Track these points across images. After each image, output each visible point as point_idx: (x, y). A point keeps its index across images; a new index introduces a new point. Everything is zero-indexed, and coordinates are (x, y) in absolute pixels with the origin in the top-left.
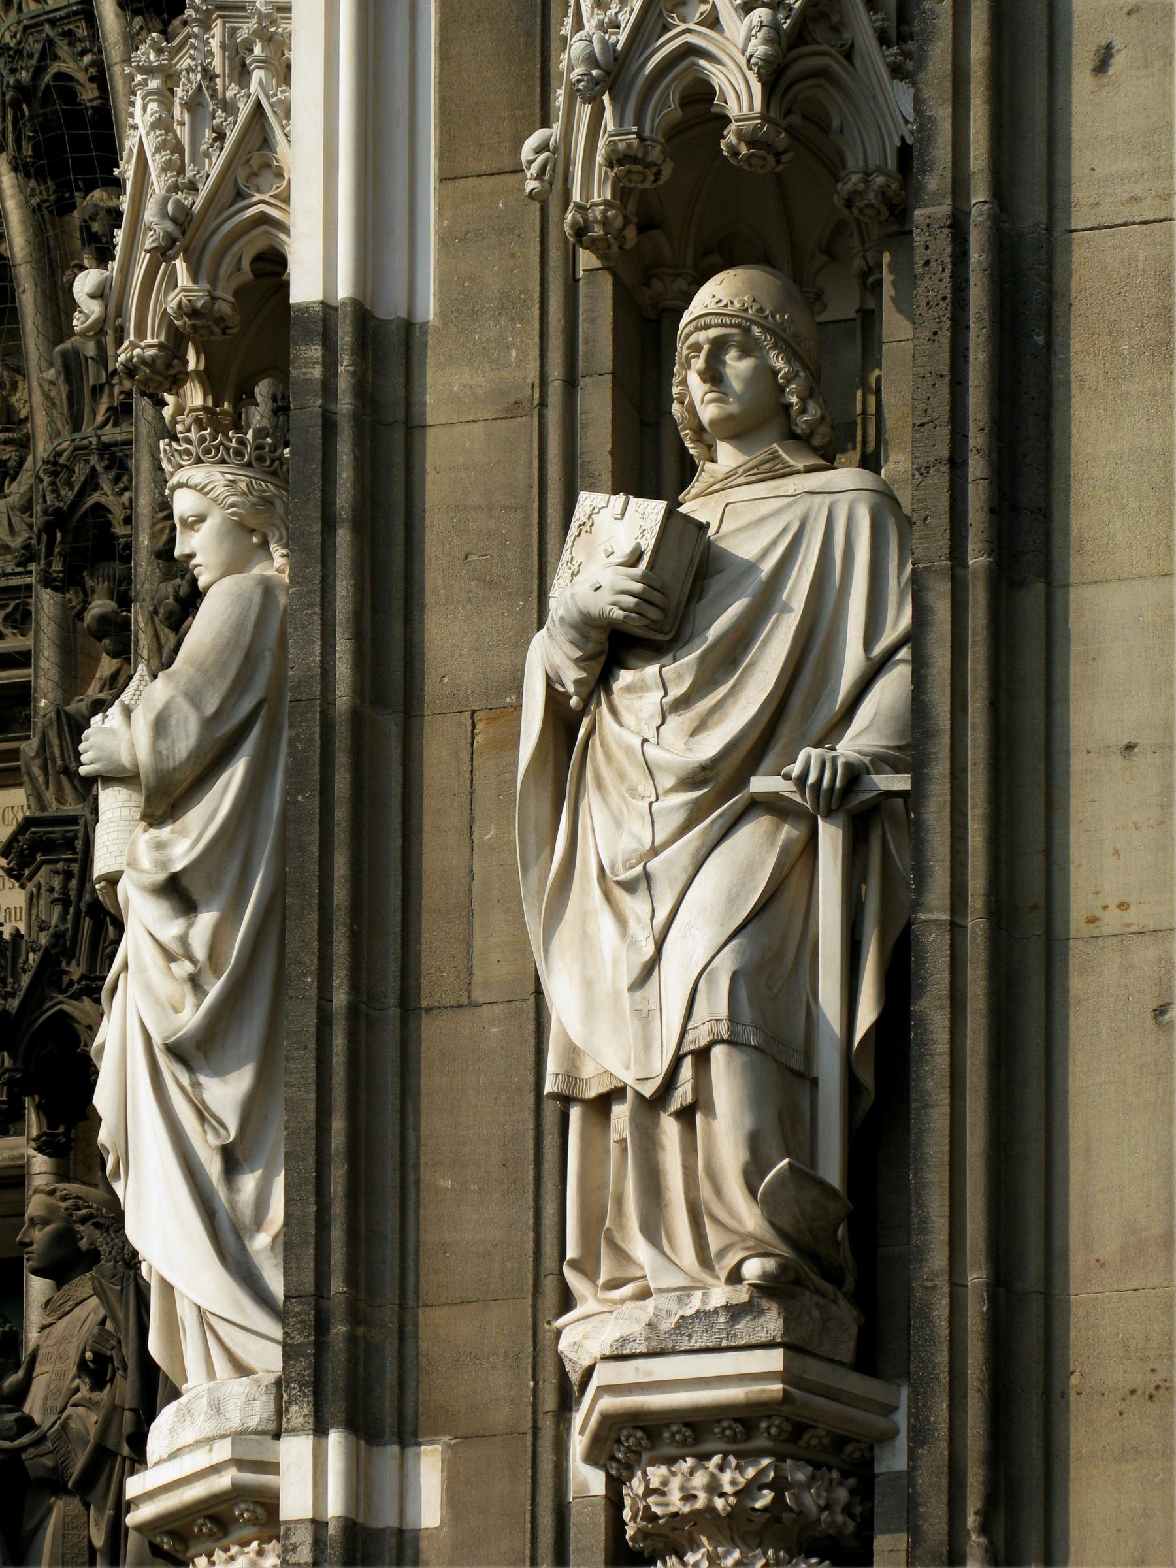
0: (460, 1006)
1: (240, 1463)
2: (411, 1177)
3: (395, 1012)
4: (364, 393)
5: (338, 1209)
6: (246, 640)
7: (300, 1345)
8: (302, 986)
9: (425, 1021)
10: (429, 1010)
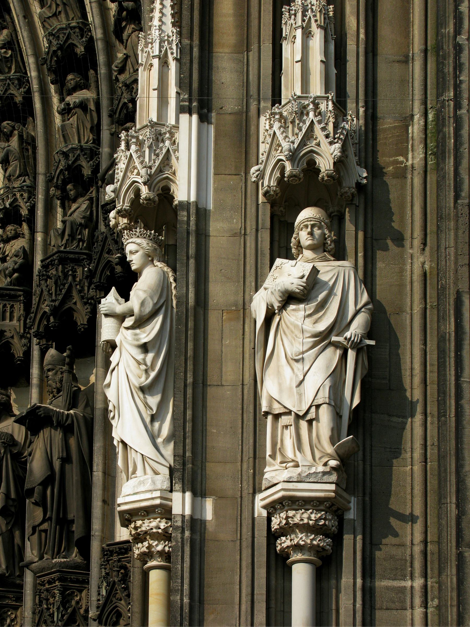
1: (161, 498)
2: (204, 428)
3: (201, 385)
4: (197, 225)
6: (161, 284)
9: (208, 388)
10: (209, 385)
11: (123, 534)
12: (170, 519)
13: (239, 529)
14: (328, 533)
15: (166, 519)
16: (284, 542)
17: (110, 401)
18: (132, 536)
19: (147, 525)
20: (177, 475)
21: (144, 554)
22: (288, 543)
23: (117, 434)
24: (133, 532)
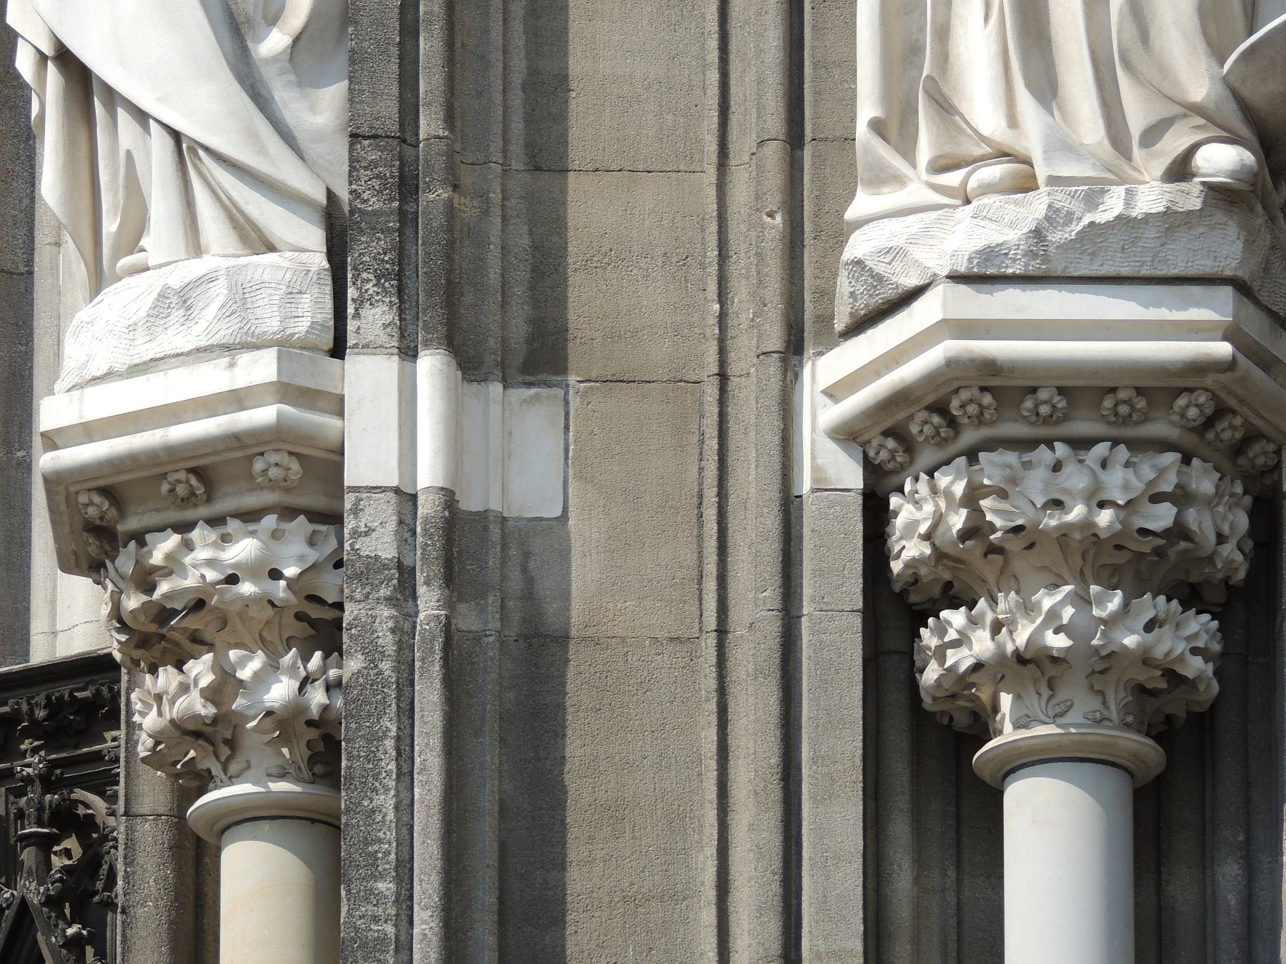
1: (285, 391)
7: (375, 213)
11: (70, 616)
12: (334, 519)
13: (711, 568)
14: (1195, 578)
15: (315, 516)
16: (959, 642)
18: (124, 627)
19: (203, 559)
20: (369, 249)
21: (190, 731)
22: (983, 644)
24: (133, 602)
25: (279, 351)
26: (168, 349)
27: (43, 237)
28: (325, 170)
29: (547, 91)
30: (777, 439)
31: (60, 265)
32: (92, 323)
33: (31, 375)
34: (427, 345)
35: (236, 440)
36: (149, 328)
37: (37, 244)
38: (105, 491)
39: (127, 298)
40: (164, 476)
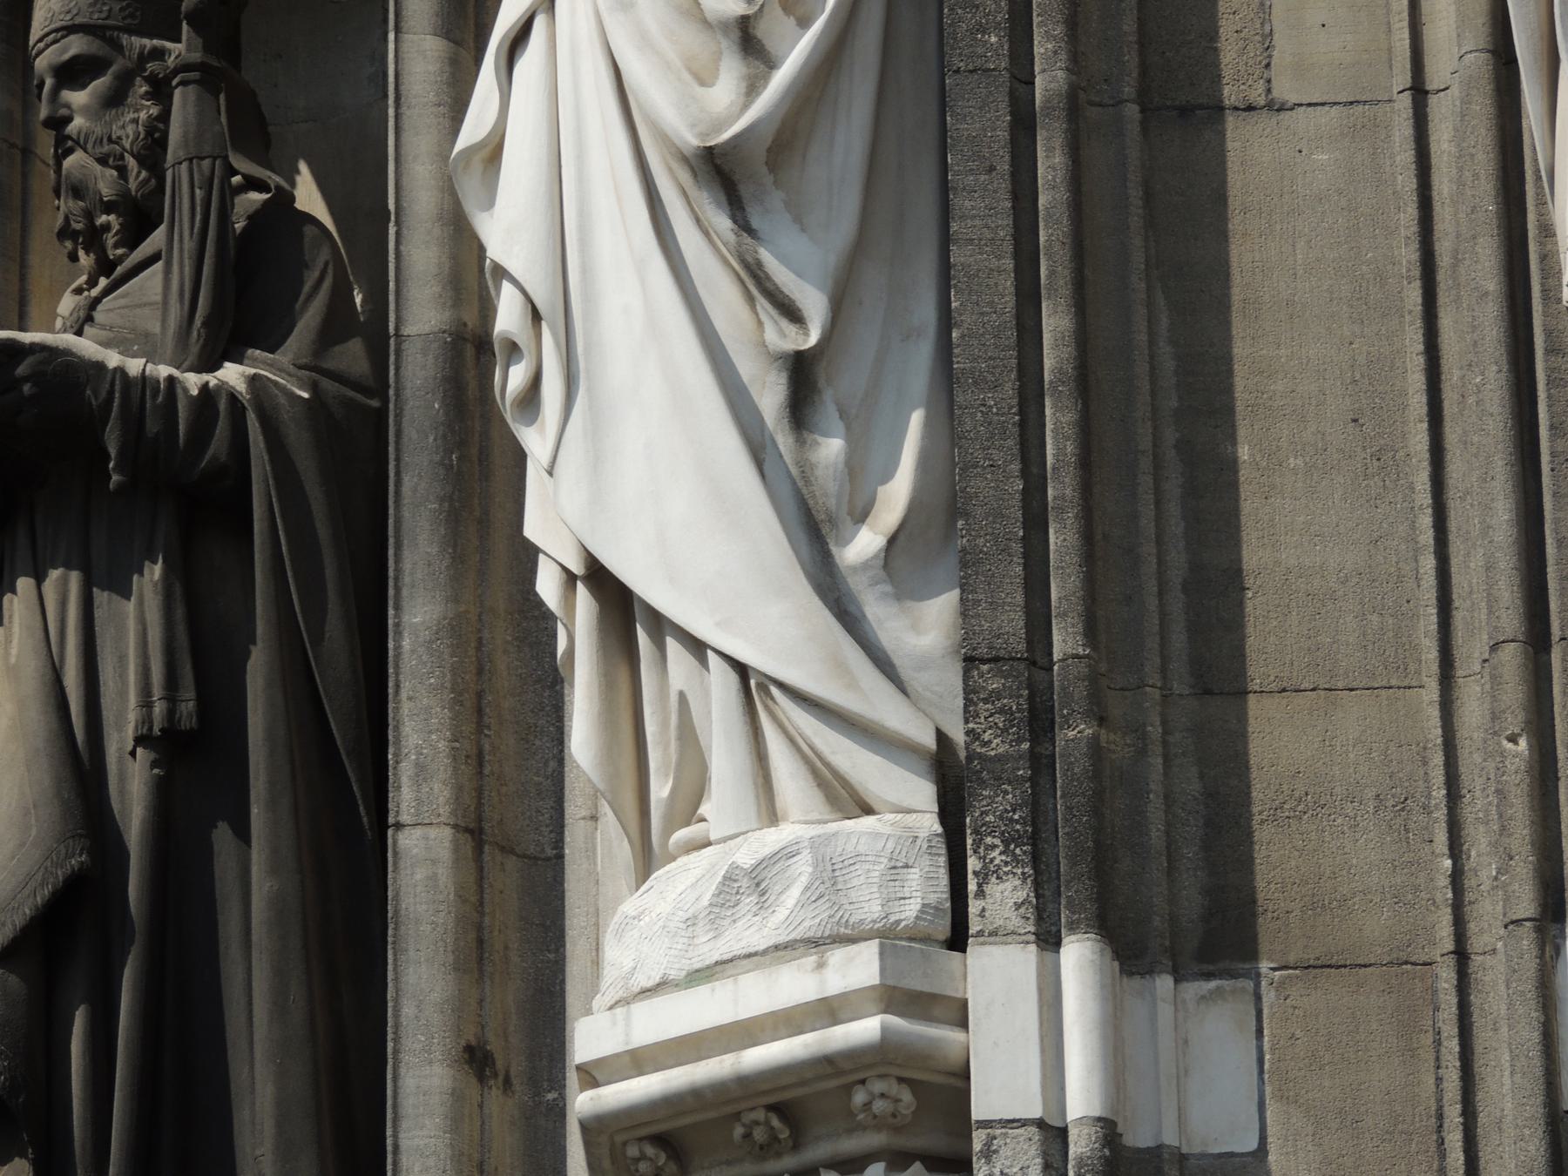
0: (1250, 108)
1: (893, 998)
5: (1060, 489)
7: (999, 758)
8: (980, 51)
17: (500, 272)
20: (994, 805)
23: (554, 520)
25: (882, 946)
26: (738, 948)
27: (575, 808)
28: (933, 708)
29: (1216, 593)
30: (1536, 1036)
31: (596, 844)
32: (637, 918)
33: (563, 991)
34: (1073, 928)
35: (829, 1064)
36: (712, 922)
37: (568, 820)
38: (660, 1140)
39: (684, 881)
40: (737, 1116)
